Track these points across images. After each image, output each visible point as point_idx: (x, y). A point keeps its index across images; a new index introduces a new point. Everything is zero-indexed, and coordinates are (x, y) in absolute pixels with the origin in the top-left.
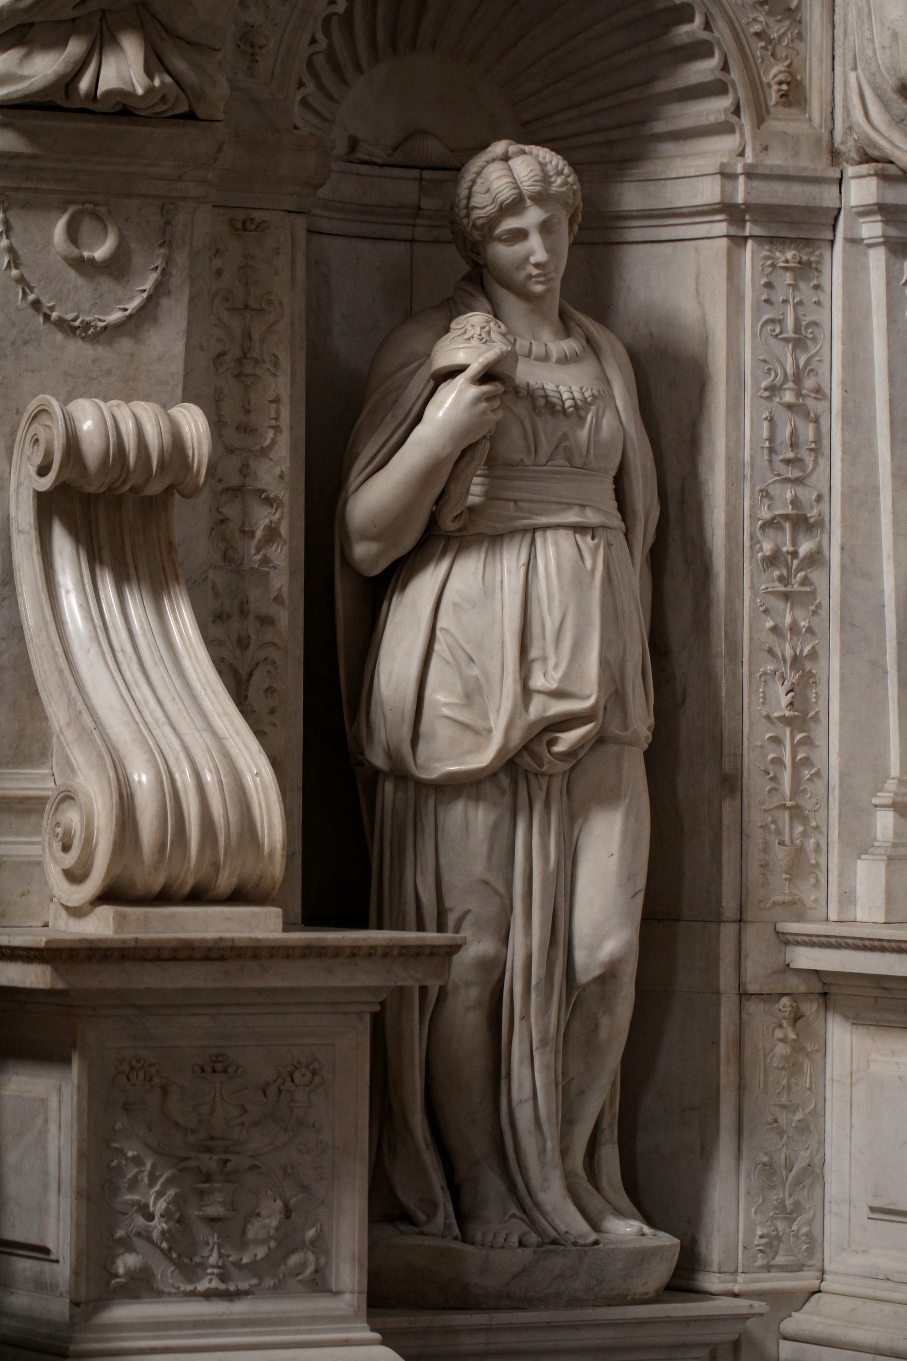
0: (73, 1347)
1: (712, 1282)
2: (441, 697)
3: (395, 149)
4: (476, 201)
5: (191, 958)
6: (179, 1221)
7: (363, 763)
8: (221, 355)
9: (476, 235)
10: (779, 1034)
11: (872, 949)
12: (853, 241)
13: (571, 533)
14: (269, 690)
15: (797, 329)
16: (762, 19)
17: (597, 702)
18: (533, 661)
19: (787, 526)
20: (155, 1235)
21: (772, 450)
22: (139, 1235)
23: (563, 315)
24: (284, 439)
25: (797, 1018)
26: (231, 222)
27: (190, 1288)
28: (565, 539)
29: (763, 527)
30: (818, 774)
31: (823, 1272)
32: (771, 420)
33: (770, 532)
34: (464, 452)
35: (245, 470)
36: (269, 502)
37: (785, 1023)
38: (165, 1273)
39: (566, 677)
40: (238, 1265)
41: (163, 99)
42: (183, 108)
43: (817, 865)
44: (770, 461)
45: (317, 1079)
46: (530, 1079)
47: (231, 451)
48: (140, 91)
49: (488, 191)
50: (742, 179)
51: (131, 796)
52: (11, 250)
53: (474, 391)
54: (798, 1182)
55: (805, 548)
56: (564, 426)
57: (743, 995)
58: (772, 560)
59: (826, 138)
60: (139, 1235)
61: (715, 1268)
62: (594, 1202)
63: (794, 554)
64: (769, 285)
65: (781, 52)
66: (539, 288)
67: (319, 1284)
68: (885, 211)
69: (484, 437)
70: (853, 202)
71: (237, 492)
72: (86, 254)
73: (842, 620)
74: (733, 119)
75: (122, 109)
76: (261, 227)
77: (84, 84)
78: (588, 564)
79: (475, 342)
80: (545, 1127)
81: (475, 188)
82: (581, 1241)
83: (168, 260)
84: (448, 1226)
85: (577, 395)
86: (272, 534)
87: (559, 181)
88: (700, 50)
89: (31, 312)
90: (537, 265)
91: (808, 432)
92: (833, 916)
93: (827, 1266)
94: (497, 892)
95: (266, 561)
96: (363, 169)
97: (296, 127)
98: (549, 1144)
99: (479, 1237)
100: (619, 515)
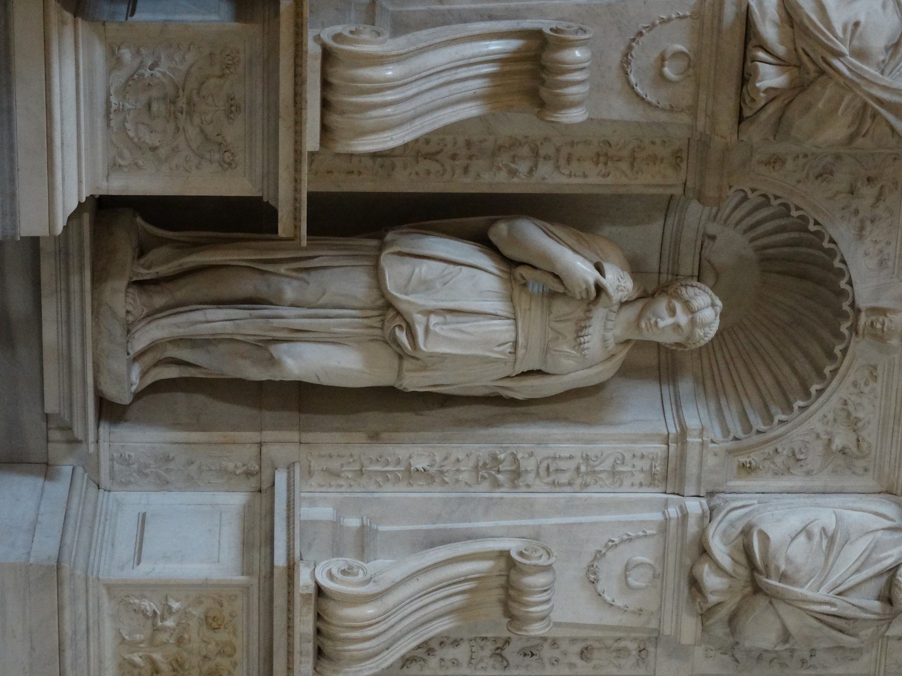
0: (80, 20)
1: (104, 429)
2: (426, 269)
3: (709, 261)
4: (690, 289)
5: (296, 84)
6: (149, 85)
7: (387, 231)
8: (610, 145)
9: (671, 290)
10: (239, 464)
11: (288, 506)
12: (666, 504)
13: (513, 339)
14: (428, 173)
16: (784, 452)
17: (423, 351)
18: (445, 317)
19: (513, 468)
20: (142, 71)
21: (554, 458)
22: (142, 62)
23: (627, 342)
24: (564, 180)
25: (248, 474)
26: (680, 150)
27: (112, 92)
28: (509, 336)
29: (513, 453)
30: (380, 486)
31: (109, 491)
32: (571, 457)
33: (510, 458)
34: (557, 276)
35: (547, 158)
36: (531, 171)
37: (245, 468)
38: (120, 77)
39: (436, 333)
40: (125, 120)
41: (753, 100)
42: (747, 113)
43: (331, 486)
44: (548, 458)
45: (226, 166)
46: (217, 320)
47: (558, 150)
48: (758, 85)
49: (696, 295)
50: (700, 440)
51: (382, 64)
52: (670, 20)
53: (591, 281)
54: (158, 476)
55: (500, 477)
56: (570, 336)
57: (261, 444)
58: (494, 458)
59: (721, 489)
60: (142, 62)
61: (113, 429)
62: (149, 359)
63: (499, 472)
64: (643, 457)
65: (767, 464)
66: (643, 325)
67: (114, 167)
68: (685, 515)
69: (566, 288)
70: (687, 503)
71: (535, 153)
72: (666, 63)
73: (462, 498)
74: (731, 437)
75: (745, 78)
76: (676, 167)
77: (761, 54)
78: (497, 349)
79: (617, 283)
80: (192, 328)
81: (697, 290)
82: (129, 345)
83: (663, 110)
84: (137, 274)
85: (586, 345)
86: (513, 173)
87: (702, 334)
88: (769, 418)
89: (636, 31)
90: (656, 323)
91: (564, 478)
92: (303, 494)
93: (112, 493)
94: (318, 300)
95: (499, 169)
96: (699, 243)
97: (730, 187)
98: (181, 330)
99: (131, 290)
100: (520, 372)
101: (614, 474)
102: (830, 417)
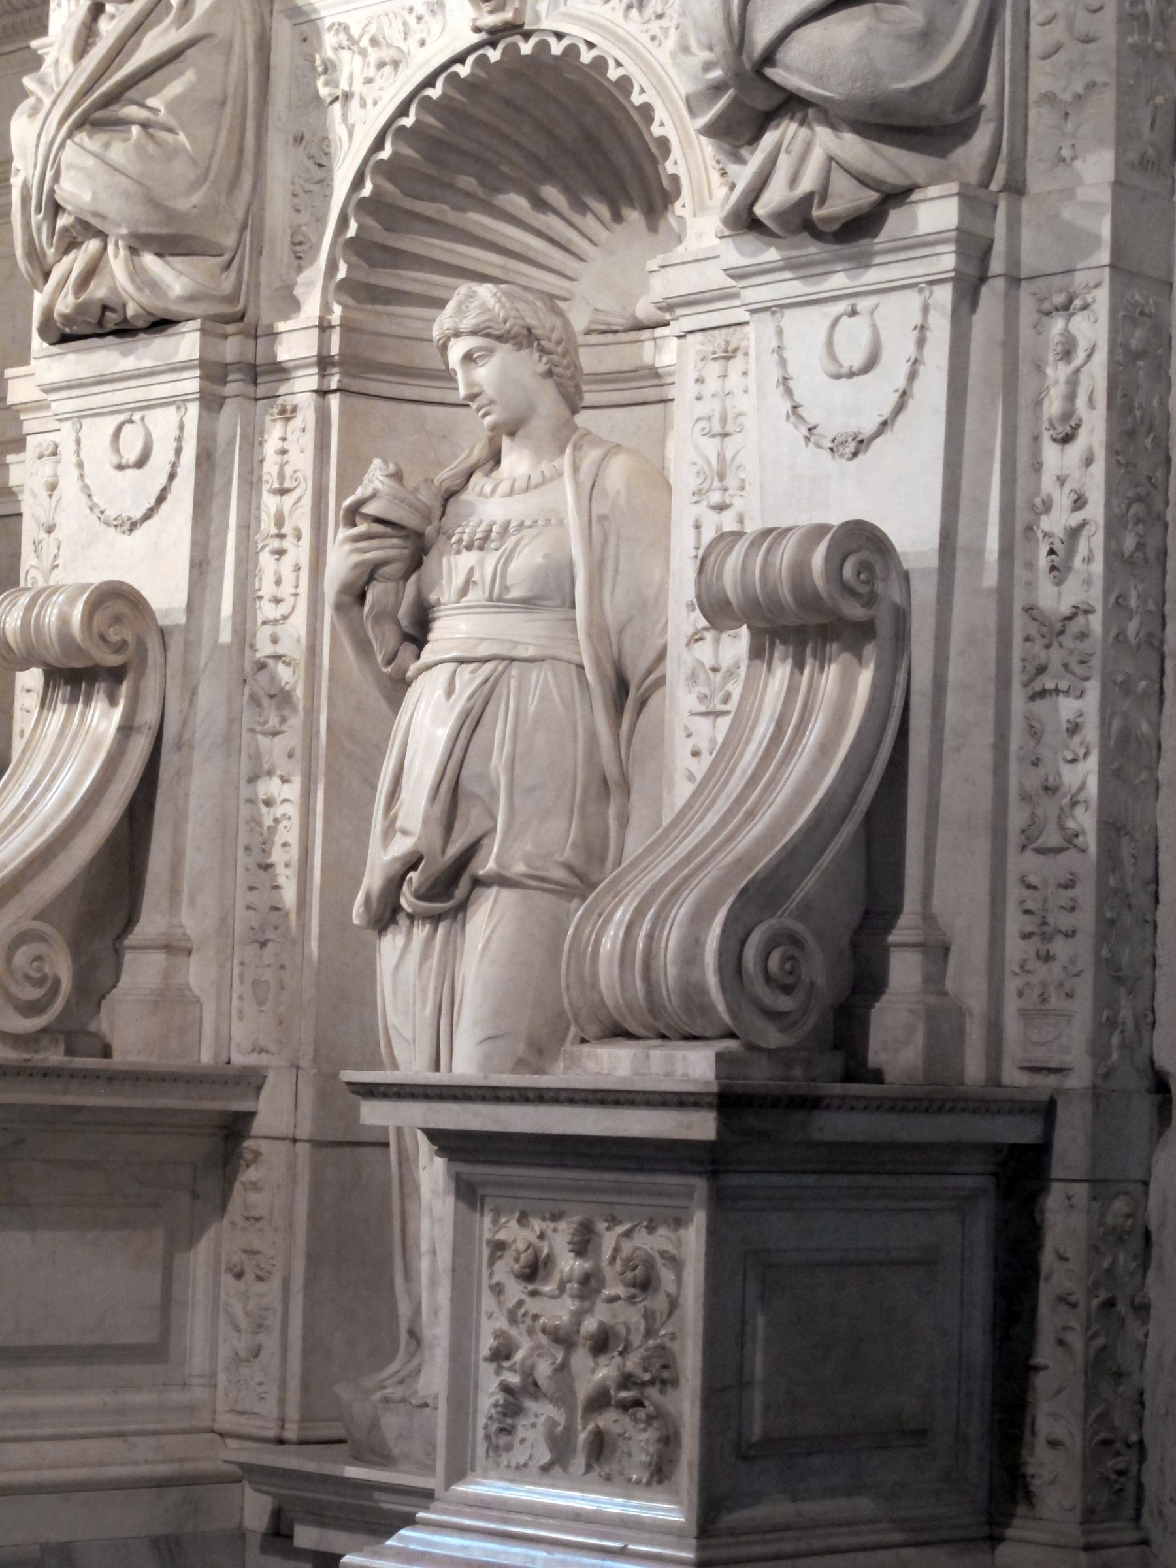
15: (724, 421)
29: (688, 644)
32: (698, 527)
64: (700, 380)
101: (725, 435)
102: (655, 27)
